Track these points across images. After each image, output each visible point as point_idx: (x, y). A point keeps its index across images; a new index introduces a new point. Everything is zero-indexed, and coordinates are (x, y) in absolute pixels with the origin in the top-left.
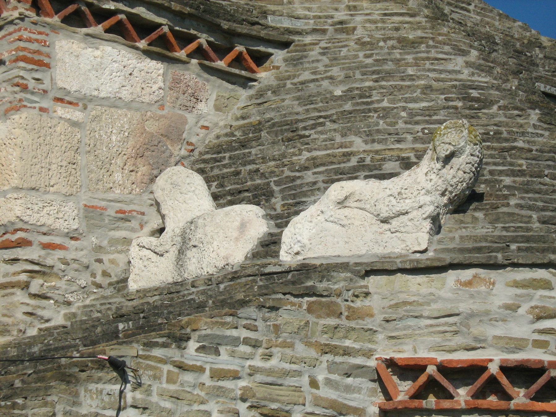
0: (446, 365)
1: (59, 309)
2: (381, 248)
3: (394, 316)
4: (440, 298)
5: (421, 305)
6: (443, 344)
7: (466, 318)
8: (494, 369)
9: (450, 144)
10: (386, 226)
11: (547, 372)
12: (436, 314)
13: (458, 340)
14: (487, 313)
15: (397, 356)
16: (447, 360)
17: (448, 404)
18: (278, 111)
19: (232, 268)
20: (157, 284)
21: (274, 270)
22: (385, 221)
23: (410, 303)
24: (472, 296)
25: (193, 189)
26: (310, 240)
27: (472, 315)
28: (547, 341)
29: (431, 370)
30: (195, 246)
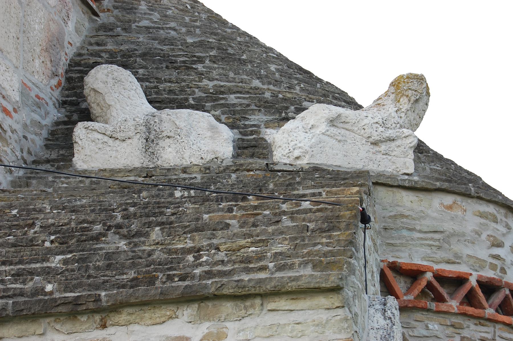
0: (440, 273)
1: (6, 175)
2: (376, 166)
3: (392, 226)
4: (427, 216)
5: (414, 220)
6: (432, 256)
7: (448, 237)
8: (473, 281)
9: (416, 91)
10: (377, 148)
11: (503, 290)
12: (425, 229)
13: (440, 255)
14: (463, 235)
15: (399, 261)
16: (441, 269)
17: (445, 307)
18: (138, 45)
19: (222, 162)
20: (120, 166)
21: (285, 169)
22: (375, 143)
23: (407, 217)
24: (452, 219)
25: (134, 88)
26: (311, 148)
27: (453, 235)
28: (496, 265)
29: (429, 276)
30: (169, 137)
